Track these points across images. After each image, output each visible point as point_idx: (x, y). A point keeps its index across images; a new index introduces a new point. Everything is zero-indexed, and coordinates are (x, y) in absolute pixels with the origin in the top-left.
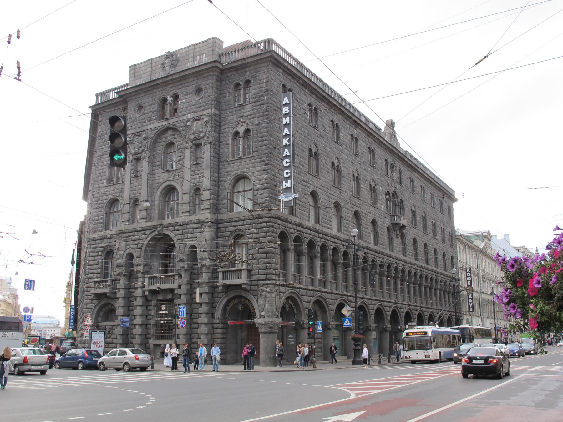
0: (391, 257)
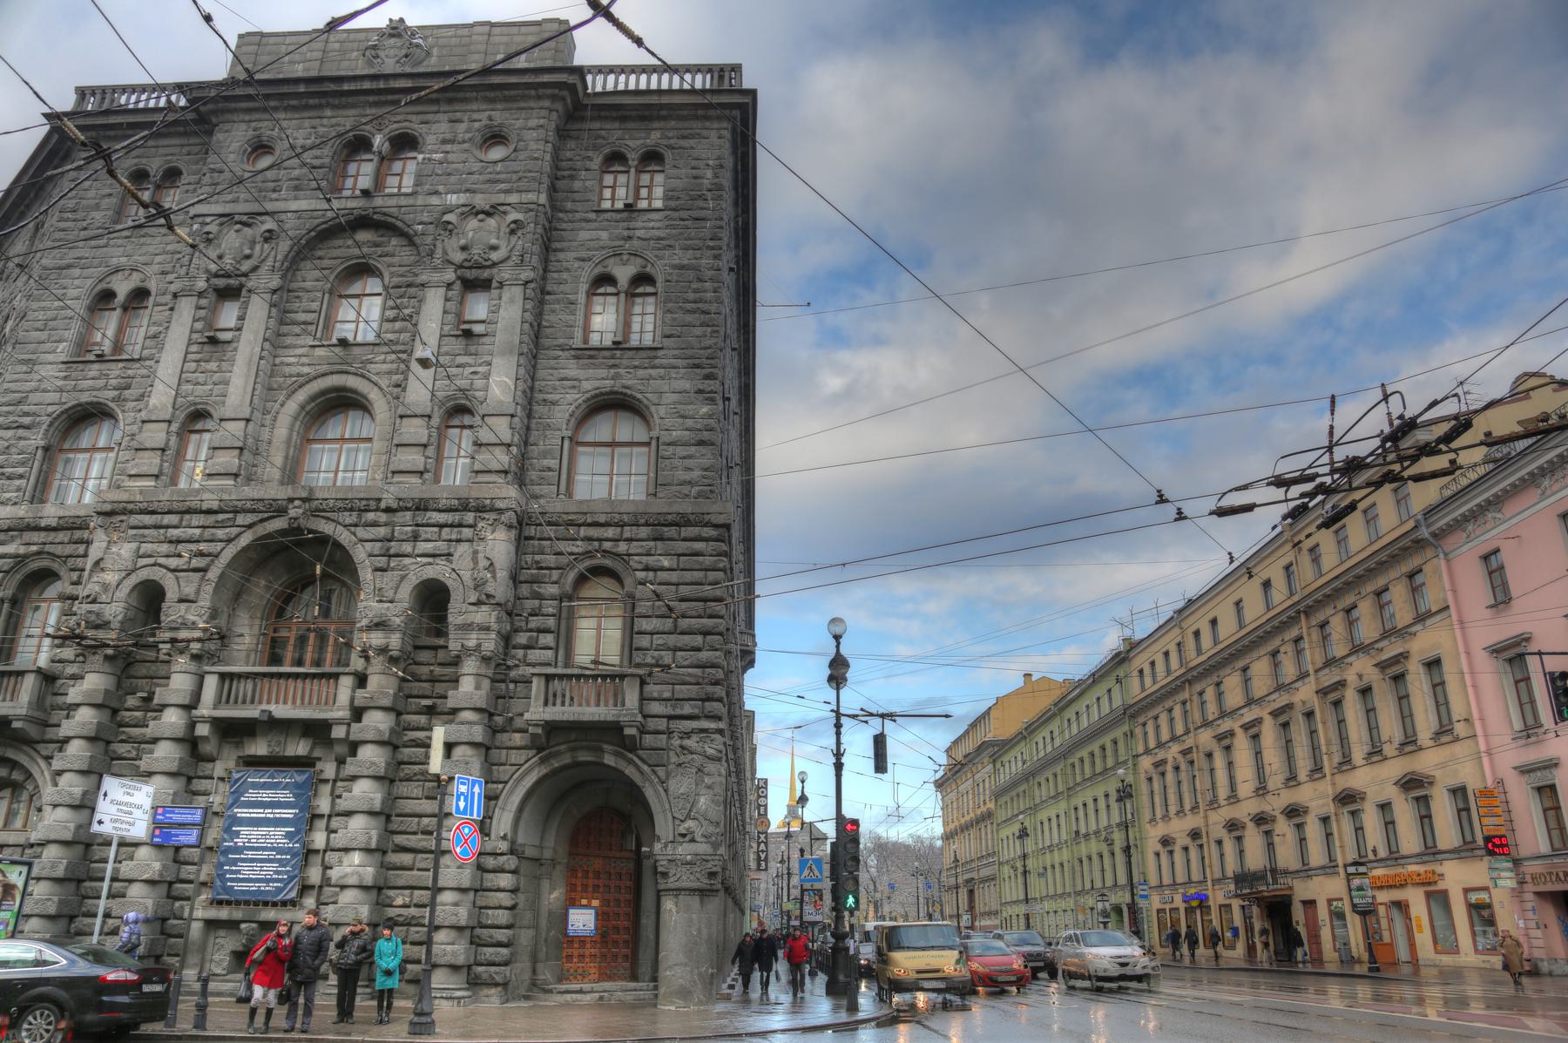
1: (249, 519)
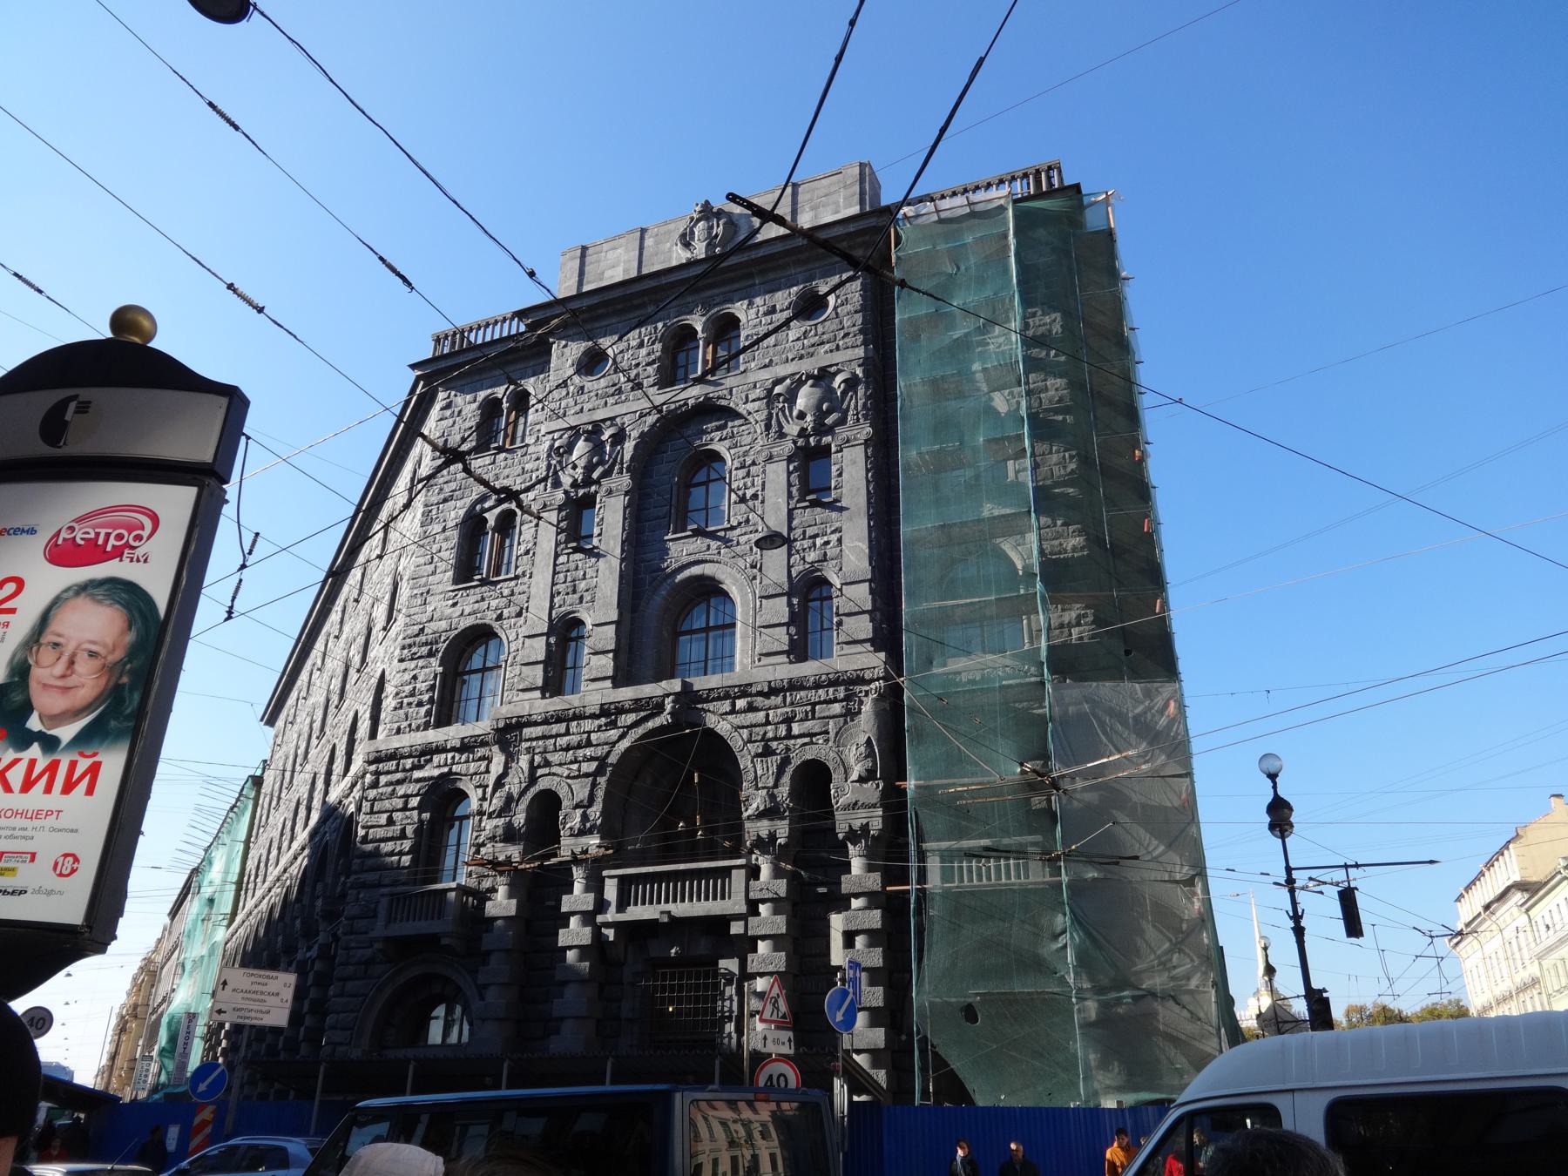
1: (631, 718)
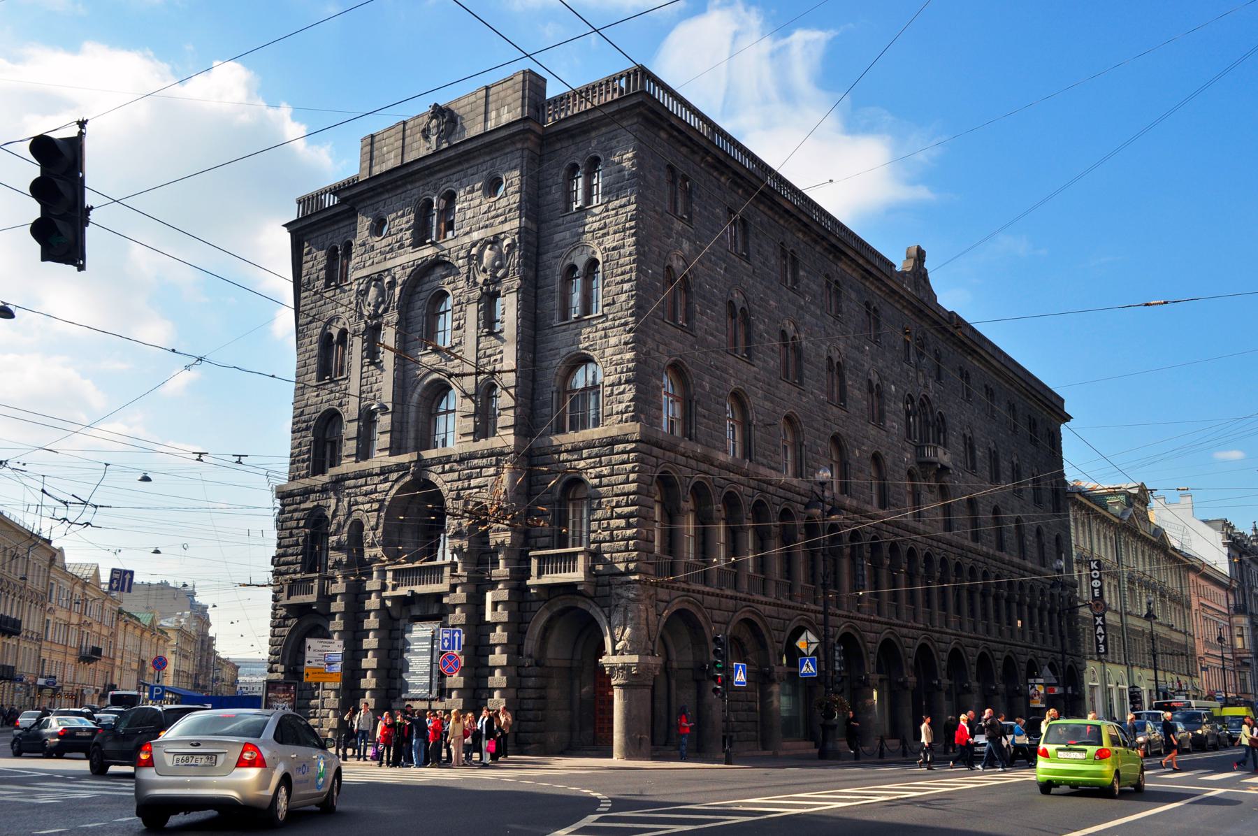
0: (915, 533)
1: (394, 476)
